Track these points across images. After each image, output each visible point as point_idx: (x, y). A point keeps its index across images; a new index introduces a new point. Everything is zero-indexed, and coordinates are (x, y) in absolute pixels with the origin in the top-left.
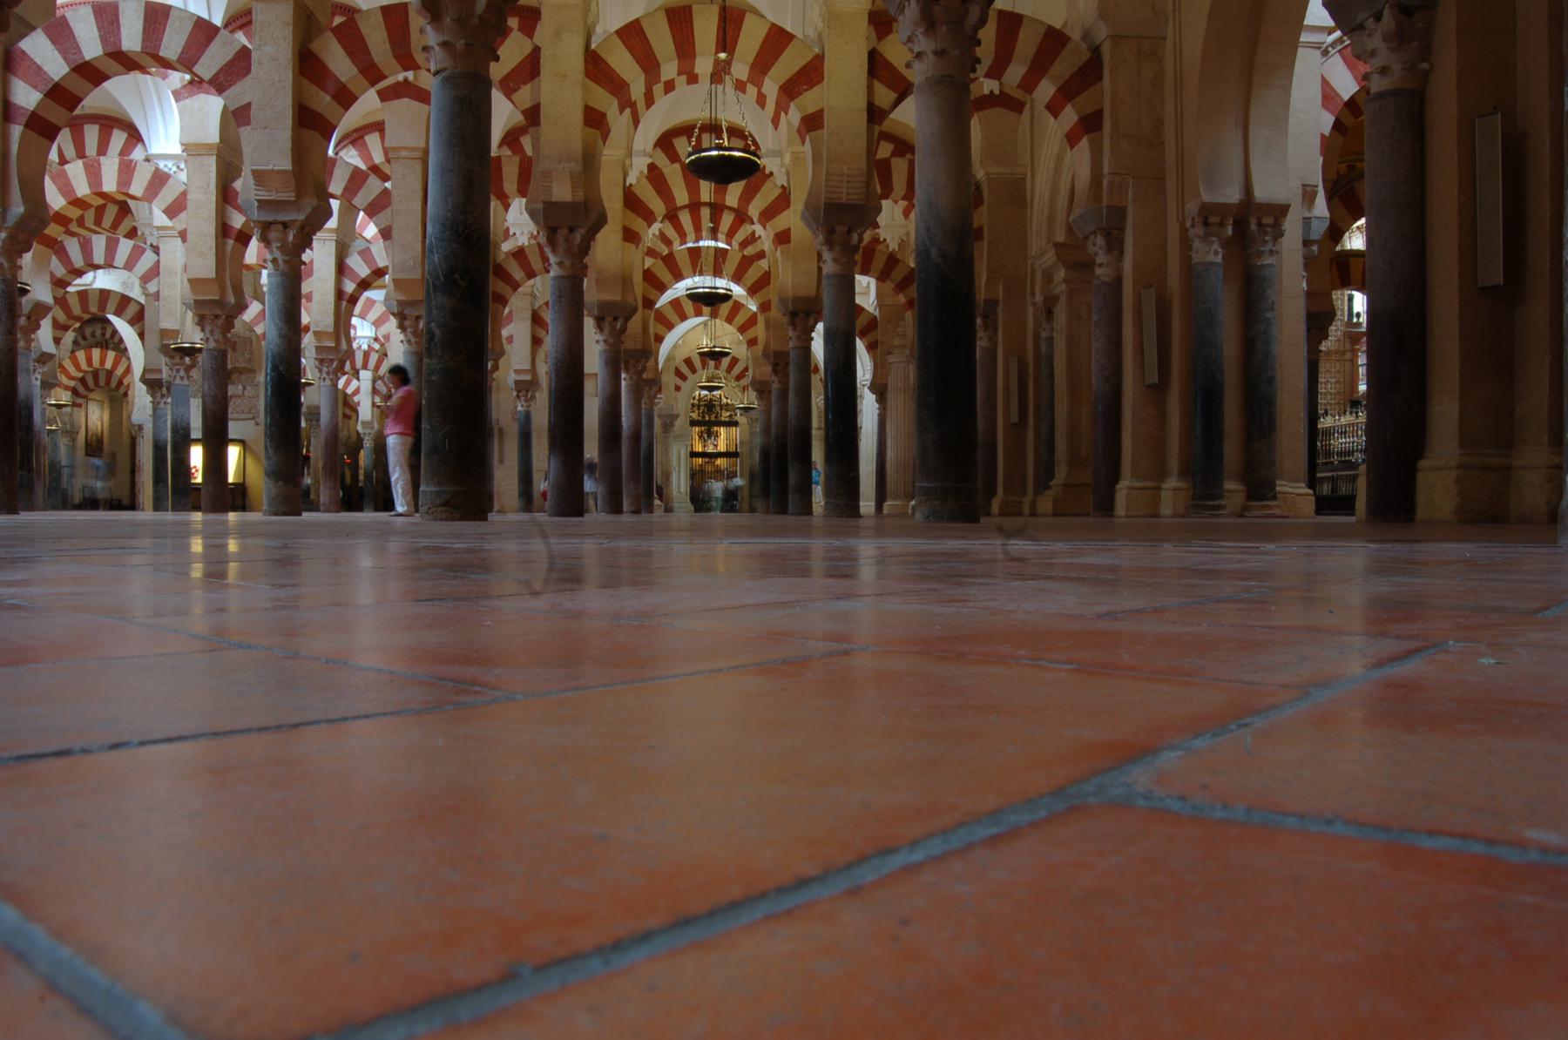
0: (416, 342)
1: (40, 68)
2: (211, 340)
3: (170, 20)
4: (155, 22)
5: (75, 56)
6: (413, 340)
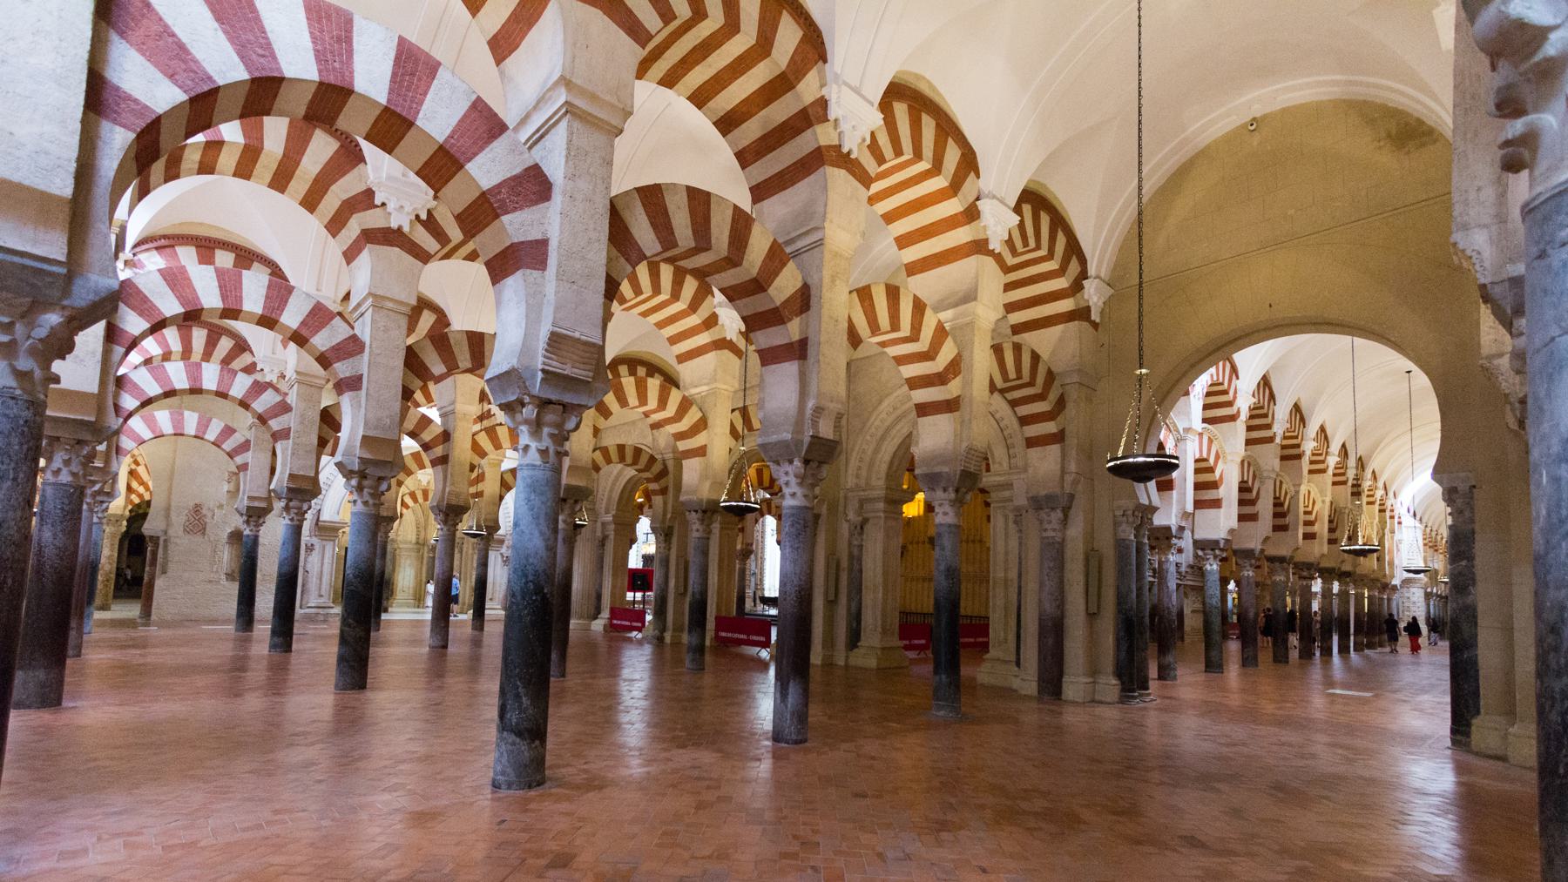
0: (374, 504)
1: (182, 47)
2: (65, 471)
3: (435, 82)
4: (413, 74)
5: (262, 60)
6: (371, 502)
